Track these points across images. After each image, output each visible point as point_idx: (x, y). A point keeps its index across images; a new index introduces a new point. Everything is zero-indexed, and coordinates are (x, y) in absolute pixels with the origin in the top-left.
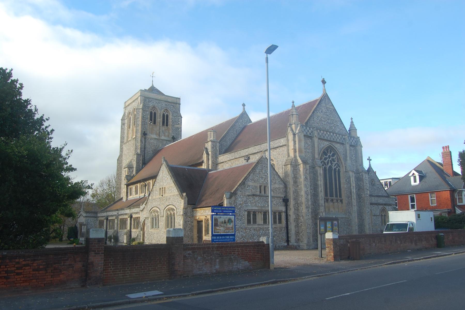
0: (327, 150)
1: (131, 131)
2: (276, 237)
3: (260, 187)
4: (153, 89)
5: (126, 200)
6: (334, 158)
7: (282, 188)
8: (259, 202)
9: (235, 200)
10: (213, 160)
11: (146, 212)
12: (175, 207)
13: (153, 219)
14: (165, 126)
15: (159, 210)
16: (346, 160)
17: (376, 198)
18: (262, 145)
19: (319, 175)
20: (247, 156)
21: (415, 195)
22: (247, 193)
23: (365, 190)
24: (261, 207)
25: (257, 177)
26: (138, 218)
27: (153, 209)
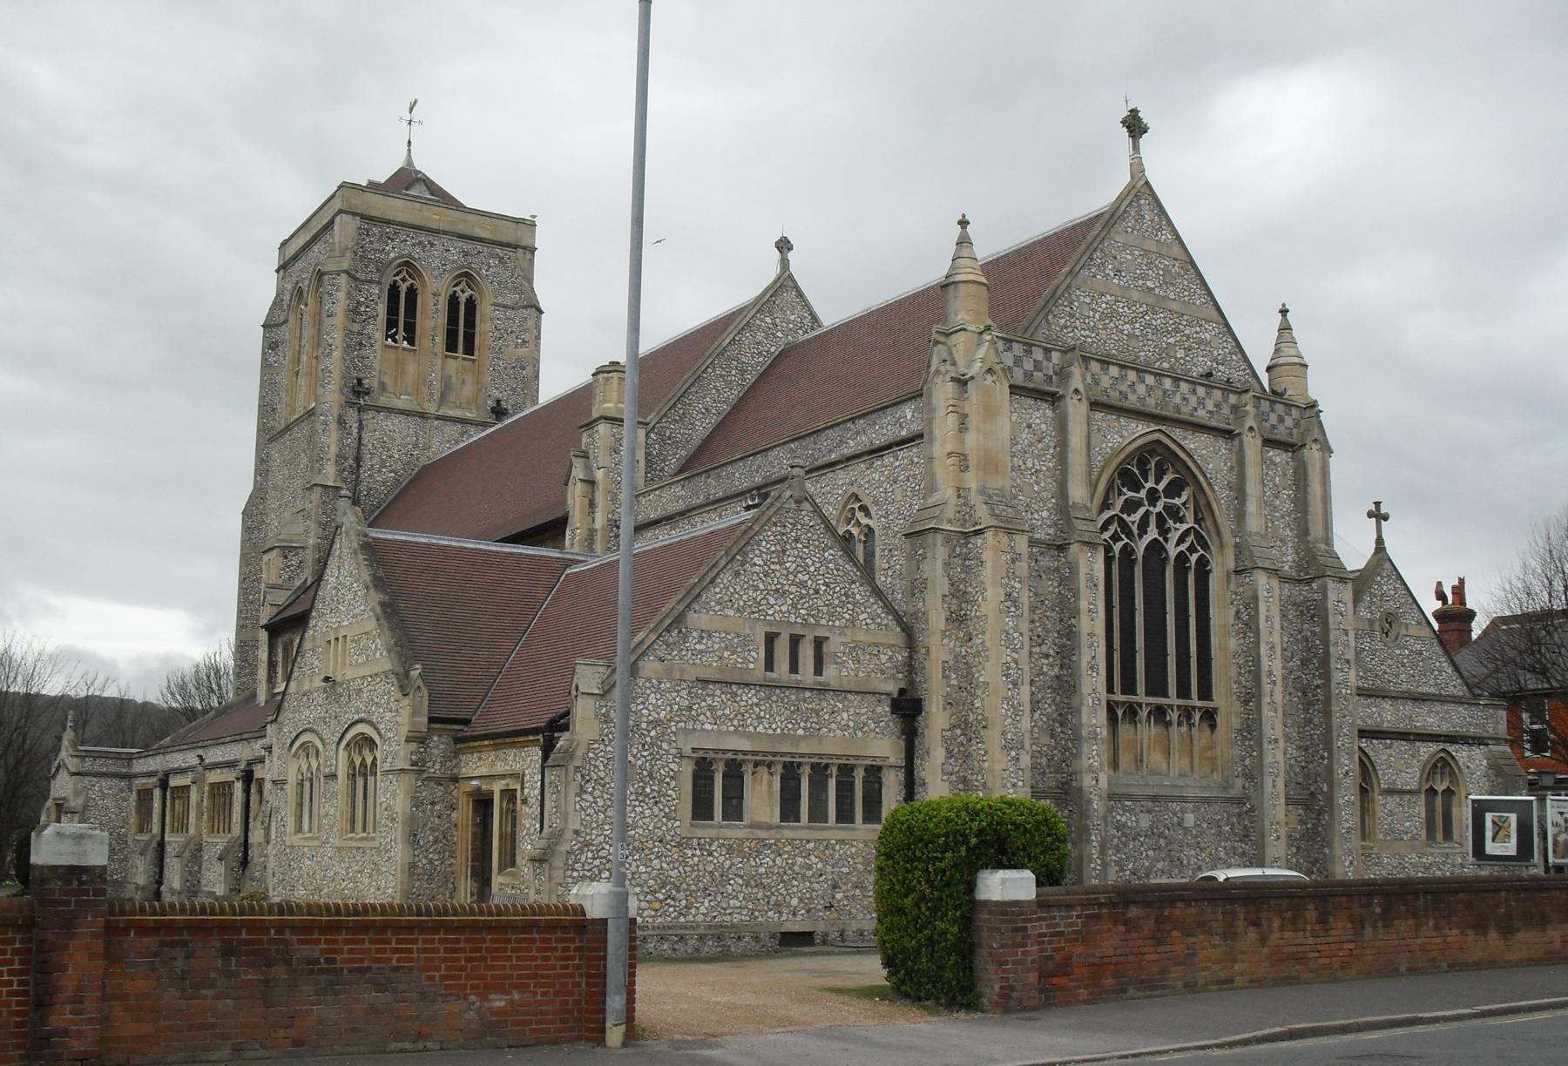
0: (1143, 464)
2: (845, 888)
3: (770, 639)
4: (407, 180)
5: (266, 702)
6: (1177, 501)
7: (890, 646)
8: (759, 717)
14: (460, 354)
16: (1240, 516)
17: (1406, 708)
19: (1082, 584)
20: (758, 489)
23: (1332, 666)
24: (773, 738)
25: (756, 589)
27: (303, 739)
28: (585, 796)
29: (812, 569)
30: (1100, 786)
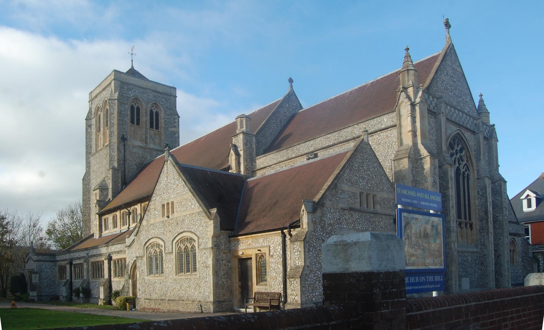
1: (101, 136)
3: (361, 194)
8: (359, 222)
9: (321, 217)
10: (247, 165)
11: (137, 248)
12: (195, 234)
13: (152, 258)
14: (154, 129)
15: (162, 243)
18: (343, 131)
21: (530, 225)
22: (341, 205)
25: (356, 176)
26: (121, 259)
28: (310, 253)
29: (371, 170)
30: (455, 247)
